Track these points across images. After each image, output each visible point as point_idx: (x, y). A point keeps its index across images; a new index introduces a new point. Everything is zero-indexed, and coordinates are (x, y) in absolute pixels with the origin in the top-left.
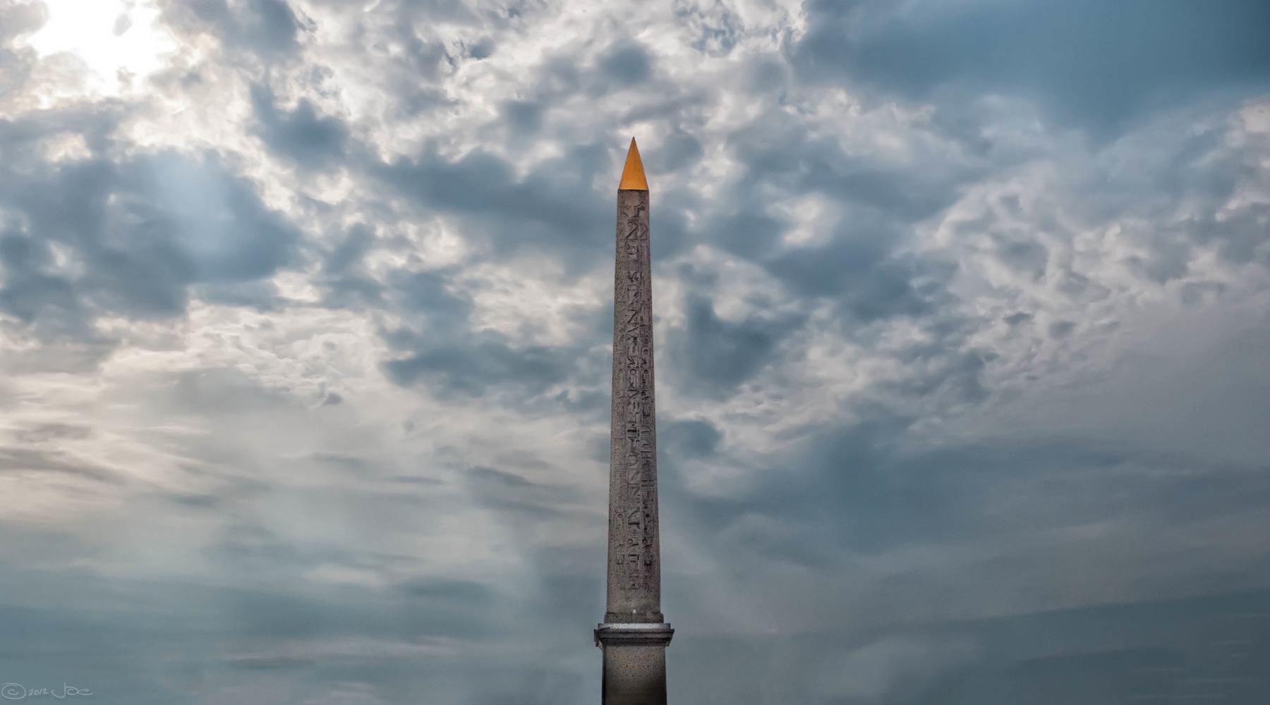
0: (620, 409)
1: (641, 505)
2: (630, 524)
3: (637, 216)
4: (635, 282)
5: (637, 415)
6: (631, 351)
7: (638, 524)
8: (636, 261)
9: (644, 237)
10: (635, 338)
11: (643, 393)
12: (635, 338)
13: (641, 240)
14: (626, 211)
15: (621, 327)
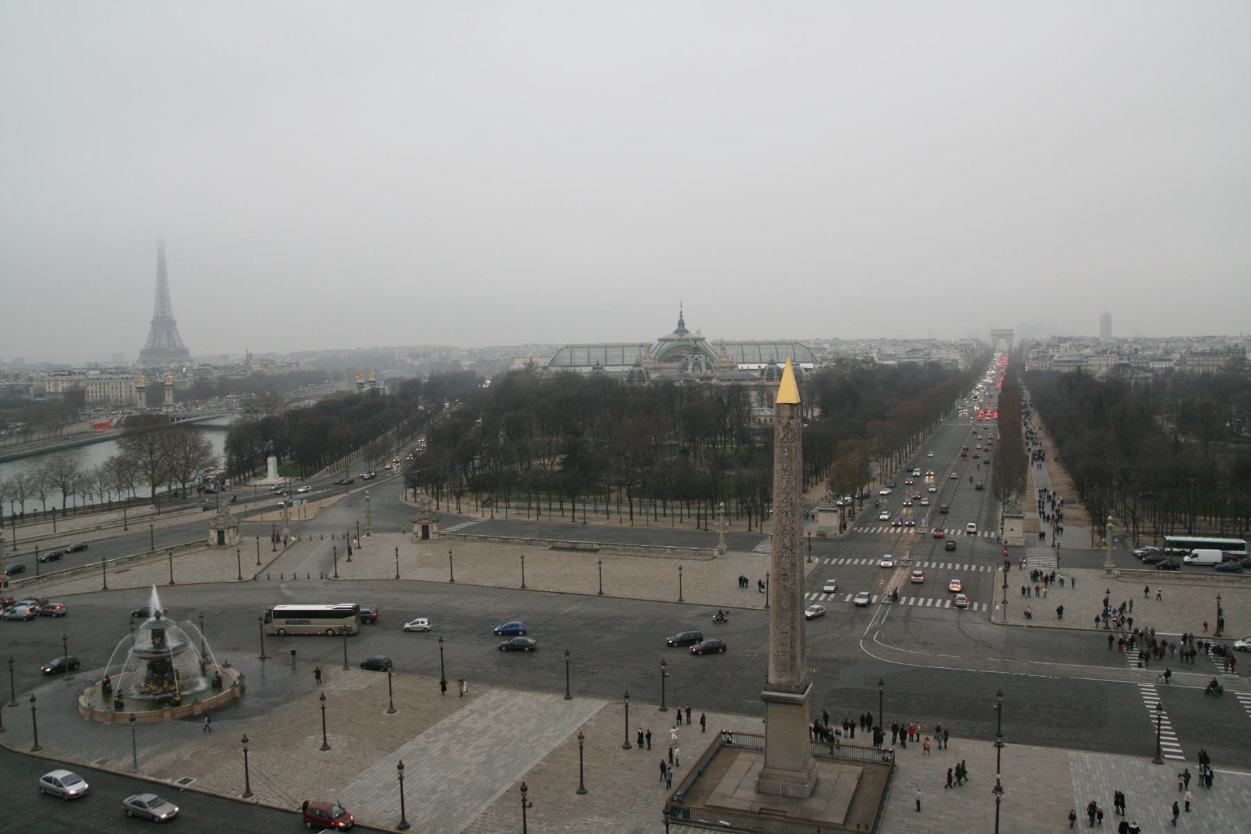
0: (777, 561)
1: (789, 622)
2: (783, 633)
3: (789, 423)
4: (787, 473)
5: (788, 565)
6: (784, 521)
7: (787, 633)
8: (787, 457)
9: (793, 440)
10: (787, 513)
11: (791, 551)
12: (787, 513)
13: (792, 442)
14: (781, 420)
15: (778, 504)
